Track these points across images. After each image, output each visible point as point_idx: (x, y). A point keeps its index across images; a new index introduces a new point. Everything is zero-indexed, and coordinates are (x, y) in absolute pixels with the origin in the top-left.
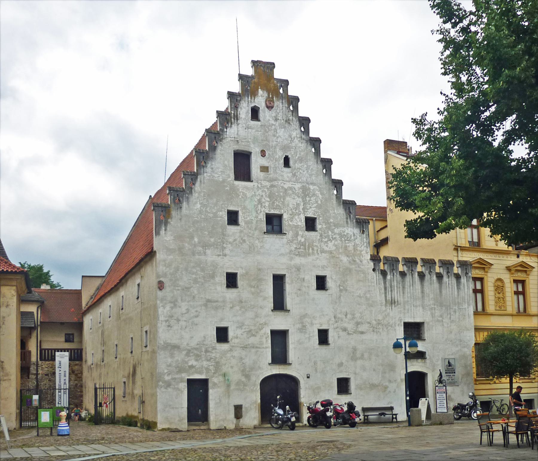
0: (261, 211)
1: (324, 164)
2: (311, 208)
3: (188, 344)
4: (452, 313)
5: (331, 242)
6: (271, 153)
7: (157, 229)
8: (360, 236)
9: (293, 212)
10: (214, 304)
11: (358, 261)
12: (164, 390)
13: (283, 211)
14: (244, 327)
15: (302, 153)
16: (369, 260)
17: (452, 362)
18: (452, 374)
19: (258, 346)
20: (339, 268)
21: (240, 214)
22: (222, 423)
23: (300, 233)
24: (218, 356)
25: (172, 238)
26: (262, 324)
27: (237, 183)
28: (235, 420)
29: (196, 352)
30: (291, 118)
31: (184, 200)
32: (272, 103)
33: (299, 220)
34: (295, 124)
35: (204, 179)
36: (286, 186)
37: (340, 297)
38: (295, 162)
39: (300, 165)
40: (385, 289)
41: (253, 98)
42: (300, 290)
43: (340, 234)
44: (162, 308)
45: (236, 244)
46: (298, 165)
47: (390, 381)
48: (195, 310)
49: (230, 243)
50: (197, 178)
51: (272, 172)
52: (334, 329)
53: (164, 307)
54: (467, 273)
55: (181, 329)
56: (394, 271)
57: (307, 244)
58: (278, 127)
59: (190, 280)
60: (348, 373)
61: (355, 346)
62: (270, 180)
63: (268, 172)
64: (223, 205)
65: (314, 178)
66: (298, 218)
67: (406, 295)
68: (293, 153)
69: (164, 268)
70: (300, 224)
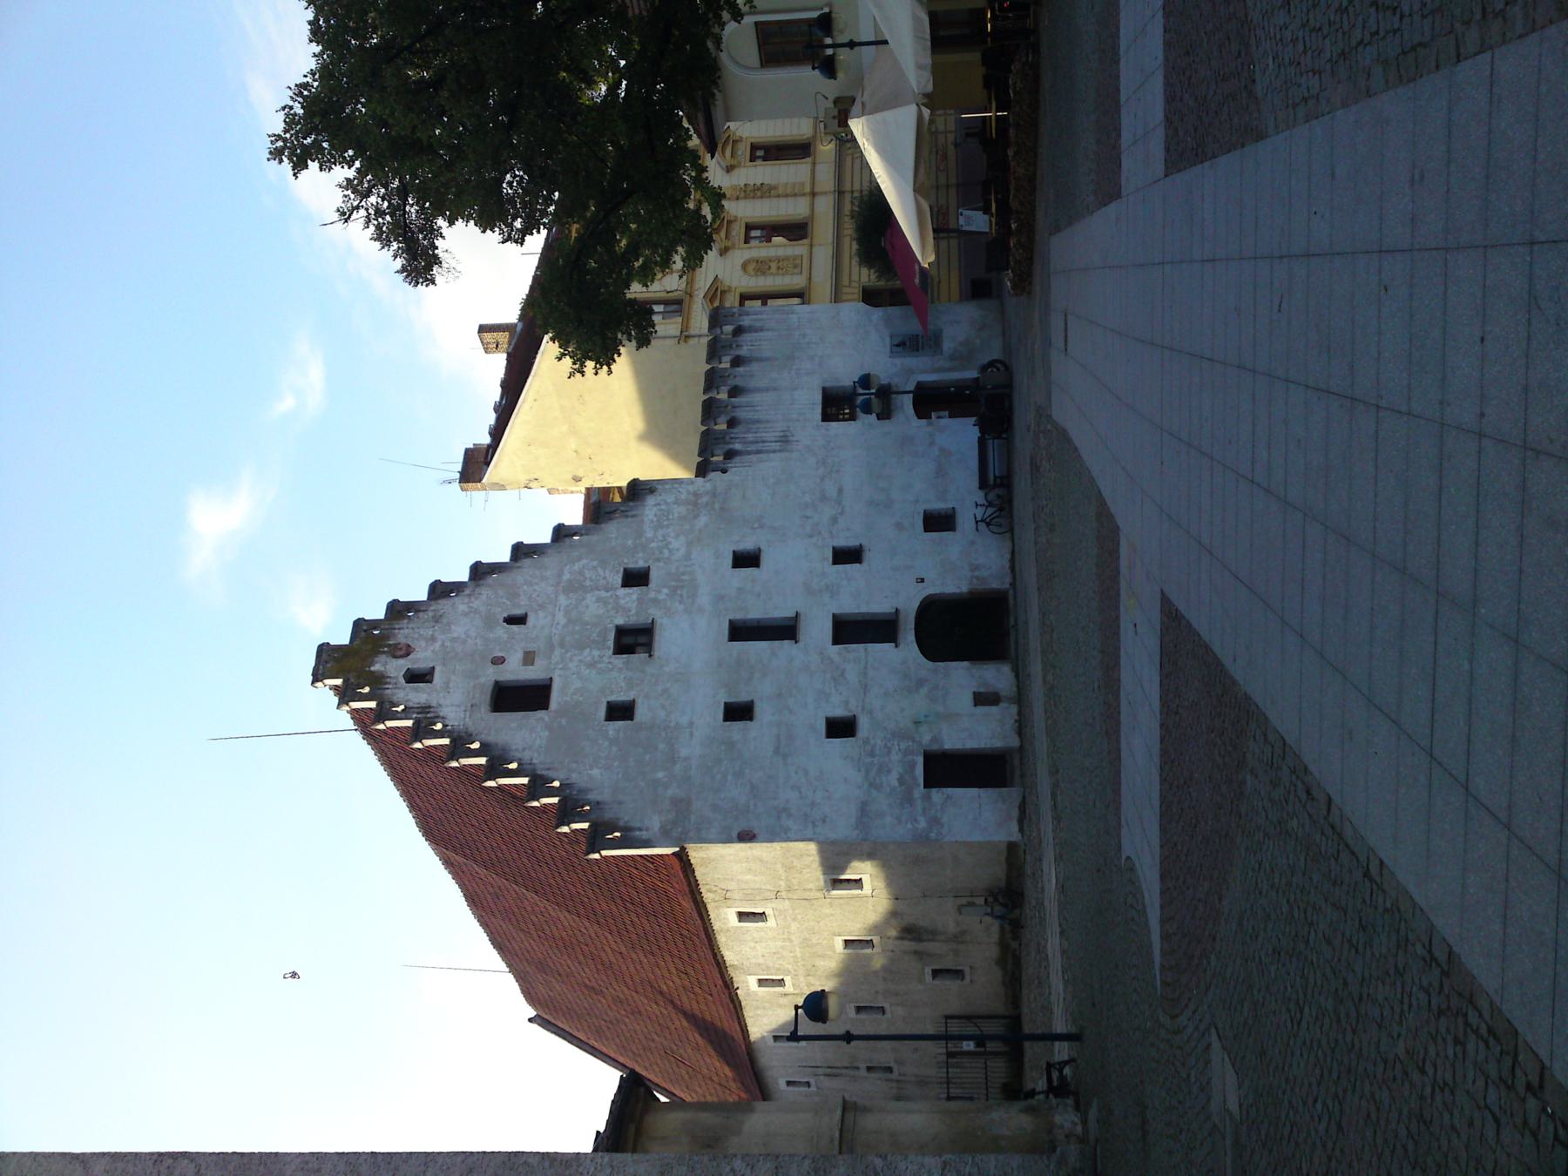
0: (609, 663)
2: (605, 578)
5: (670, 543)
6: (498, 648)
7: (638, 845)
8: (660, 495)
13: (610, 625)
16: (706, 479)
20: (719, 529)
21: (613, 698)
23: (652, 595)
27: (553, 704)
30: (431, 614)
31: (585, 797)
33: (628, 599)
34: (443, 605)
36: (563, 621)
40: (759, 452)
41: (388, 680)
42: (759, 595)
43: (656, 529)
46: (523, 601)
50: (541, 777)
51: (535, 645)
58: (448, 635)
62: (551, 647)
63: (534, 652)
65: (548, 573)
66: (623, 599)
69: (713, 830)
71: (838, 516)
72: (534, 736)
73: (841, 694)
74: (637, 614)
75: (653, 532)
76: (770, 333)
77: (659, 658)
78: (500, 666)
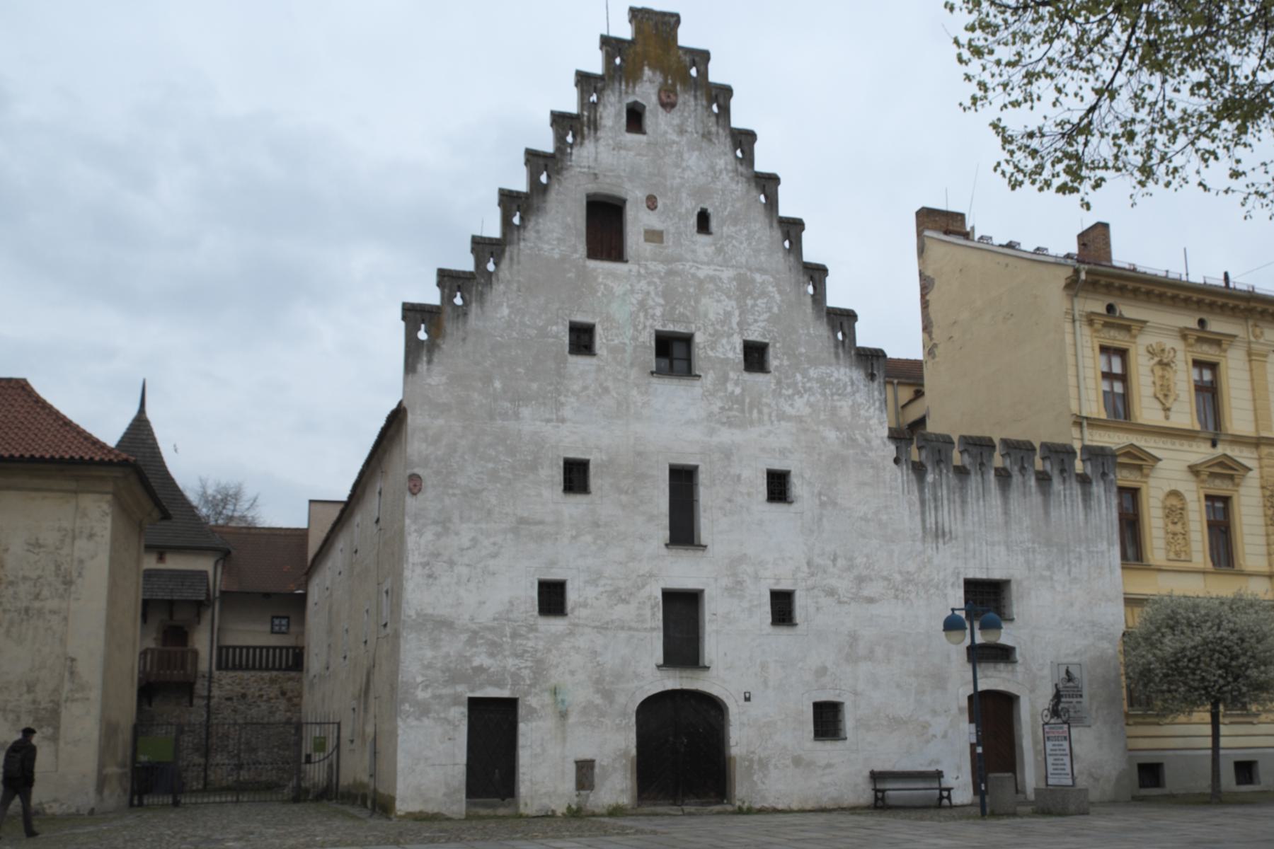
0: (645, 327)
1: (786, 229)
2: (756, 321)
3: (472, 619)
4: (1073, 562)
5: (801, 397)
6: (668, 202)
7: (410, 360)
9: (716, 331)
10: (535, 529)
11: (861, 440)
12: (414, 723)
14: (602, 582)
15: (738, 205)
16: (886, 440)
17: (1075, 671)
18: (1075, 700)
19: (633, 625)
20: (820, 454)
21: (599, 331)
22: (546, 801)
23: (732, 375)
24: (541, 645)
25: (444, 379)
26: (643, 575)
27: (592, 264)
29: (490, 637)
30: (714, 129)
31: (474, 299)
32: (672, 95)
33: (728, 348)
34: (724, 143)
35: (518, 254)
36: (701, 274)
37: (820, 519)
39: (733, 229)
40: (923, 502)
41: (631, 85)
42: (730, 501)
43: (821, 380)
44: (415, 534)
45: (588, 396)
47: (934, 713)
48: (492, 540)
49: (574, 393)
50: (503, 252)
51: (671, 244)
52: (808, 590)
53: (420, 533)
54: (1104, 475)
55: (457, 583)
56: (942, 466)
57: (747, 400)
58: (685, 149)
59: (482, 472)
60: (838, 692)
61: (855, 631)
62: (667, 260)
64: (560, 311)
65: (763, 258)
66: (729, 342)
67: (970, 517)
68: (717, 204)
69: (424, 446)
70: (731, 355)
71: (836, 597)
73: (597, 599)
74: (708, 358)
75: (815, 376)
76: (1081, 517)
77: (649, 383)
78: (645, 205)
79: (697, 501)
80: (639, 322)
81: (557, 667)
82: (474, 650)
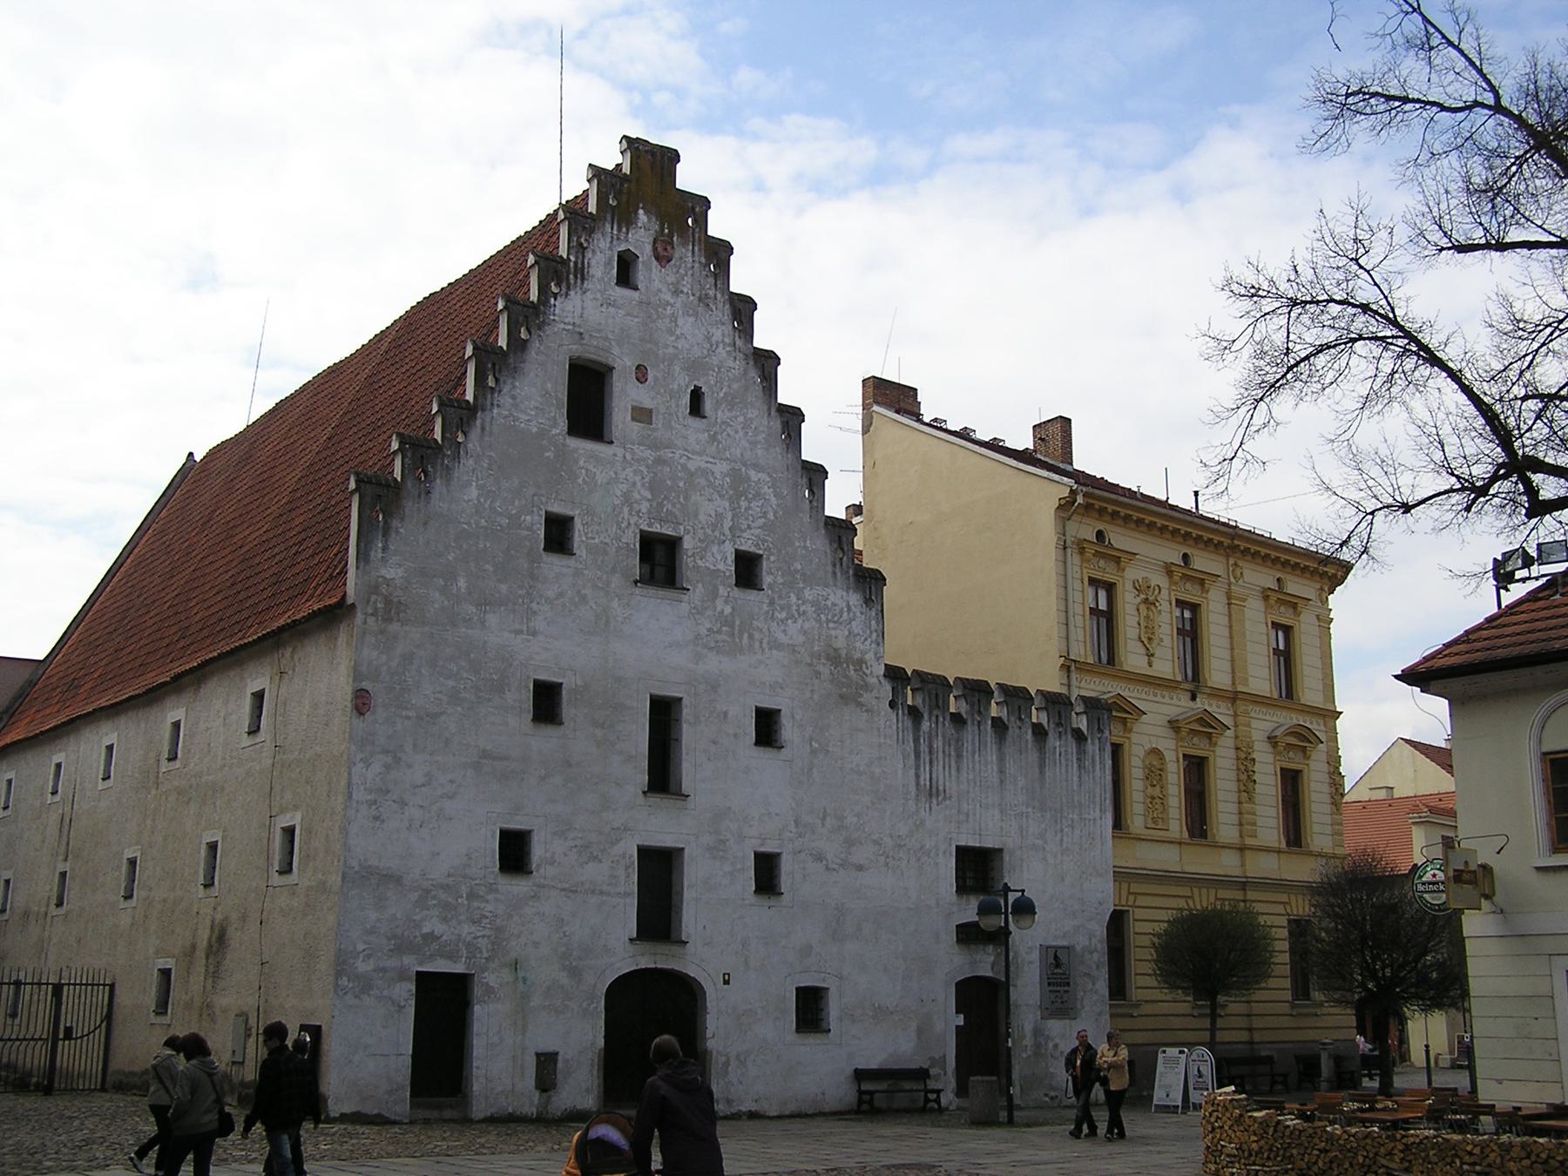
0: (629, 524)
2: (749, 527)
8: (862, 613)
13: (682, 528)
19: (605, 888)
23: (722, 591)
26: (619, 828)
28: (537, 1094)
29: (443, 896)
36: (692, 466)
37: (811, 769)
38: (718, 403)
42: (714, 743)
46: (723, 415)
51: (660, 425)
62: (656, 446)
65: (759, 452)
66: (719, 551)
70: (721, 566)
72: (533, 413)
74: (696, 568)
79: (678, 740)
80: (623, 518)
81: (519, 936)
82: (425, 912)
